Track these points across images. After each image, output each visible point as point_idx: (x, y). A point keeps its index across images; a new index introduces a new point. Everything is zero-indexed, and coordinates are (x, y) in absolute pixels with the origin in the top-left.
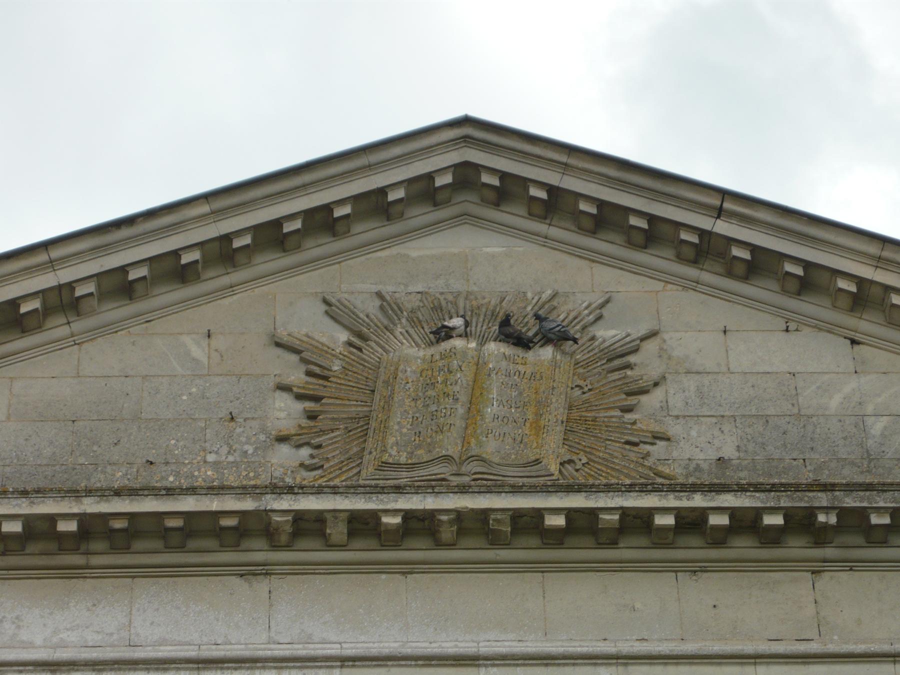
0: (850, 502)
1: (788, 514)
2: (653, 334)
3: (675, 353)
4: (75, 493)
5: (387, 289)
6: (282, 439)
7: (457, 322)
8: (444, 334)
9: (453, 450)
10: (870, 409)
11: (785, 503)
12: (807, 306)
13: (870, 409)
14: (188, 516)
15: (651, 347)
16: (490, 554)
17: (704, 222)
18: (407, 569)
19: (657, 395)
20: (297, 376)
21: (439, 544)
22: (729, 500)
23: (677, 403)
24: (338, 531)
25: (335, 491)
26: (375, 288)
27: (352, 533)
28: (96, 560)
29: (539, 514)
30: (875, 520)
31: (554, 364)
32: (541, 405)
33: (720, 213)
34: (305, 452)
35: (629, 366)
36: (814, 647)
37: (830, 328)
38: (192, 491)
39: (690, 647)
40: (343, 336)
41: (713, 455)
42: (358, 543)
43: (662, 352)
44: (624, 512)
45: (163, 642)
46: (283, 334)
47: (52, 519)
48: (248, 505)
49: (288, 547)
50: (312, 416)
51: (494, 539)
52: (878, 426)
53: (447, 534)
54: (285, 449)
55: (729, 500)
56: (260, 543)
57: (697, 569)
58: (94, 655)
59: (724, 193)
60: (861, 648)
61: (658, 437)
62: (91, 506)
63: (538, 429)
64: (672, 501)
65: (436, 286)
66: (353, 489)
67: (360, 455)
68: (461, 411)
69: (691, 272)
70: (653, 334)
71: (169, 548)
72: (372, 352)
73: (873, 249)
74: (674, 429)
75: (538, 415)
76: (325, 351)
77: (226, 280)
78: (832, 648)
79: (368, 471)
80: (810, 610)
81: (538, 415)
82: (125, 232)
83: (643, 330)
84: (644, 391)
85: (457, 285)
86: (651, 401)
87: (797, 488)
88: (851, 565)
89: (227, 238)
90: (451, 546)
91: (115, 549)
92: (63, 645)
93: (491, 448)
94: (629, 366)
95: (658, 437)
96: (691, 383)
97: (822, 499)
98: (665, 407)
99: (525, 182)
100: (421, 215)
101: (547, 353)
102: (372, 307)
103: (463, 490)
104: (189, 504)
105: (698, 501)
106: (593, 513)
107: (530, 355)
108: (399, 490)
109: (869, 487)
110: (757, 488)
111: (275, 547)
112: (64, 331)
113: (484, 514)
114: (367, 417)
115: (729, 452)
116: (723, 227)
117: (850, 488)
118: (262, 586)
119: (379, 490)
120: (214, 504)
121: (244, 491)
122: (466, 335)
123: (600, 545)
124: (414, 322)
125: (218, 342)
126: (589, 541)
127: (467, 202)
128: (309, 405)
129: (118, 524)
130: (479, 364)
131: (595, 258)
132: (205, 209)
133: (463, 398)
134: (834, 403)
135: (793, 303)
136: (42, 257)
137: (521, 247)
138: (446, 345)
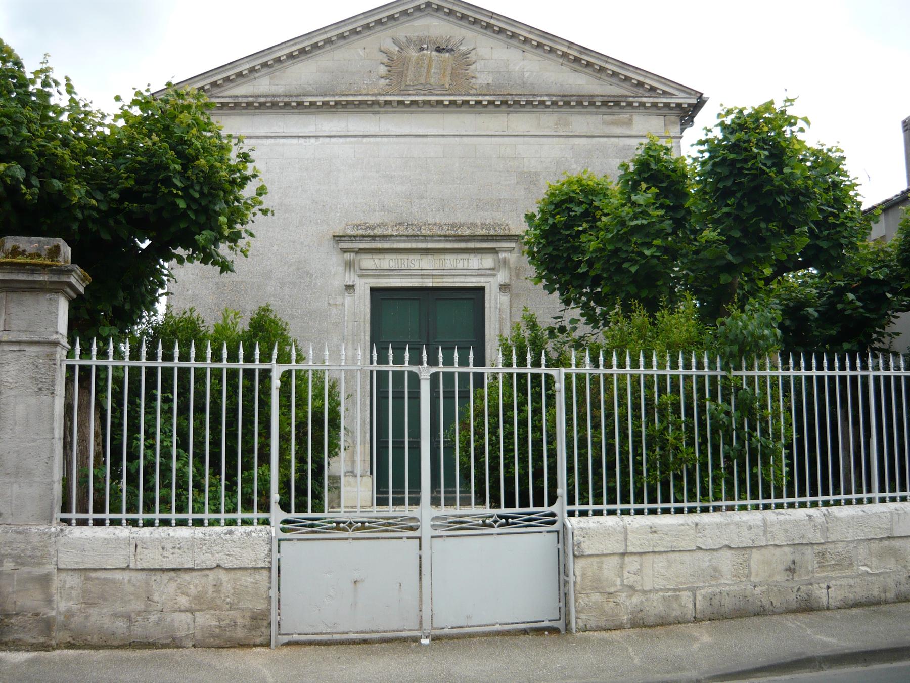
0: (516, 98)
1: (502, 102)
2: (474, 49)
3: (480, 54)
4: (333, 95)
5: (408, 35)
6: (382, 78)
7: (425, 46)
8: (422, 49)
9: (423, 82)
10: (525, 70)
11: (501, 99)
12: (513, 42)
13: (525, 70)
14: (360, 101)
15: (473, 52)
16: (431, 109)
17: (488, 20)
18: (412, 112)
19: (474, 66)
20: (385, 60)
21: (419, 107)
22: (488, 98)
23: (479, 68)
24: (395, 104)
25: (394, 95)
26: (404, 35)
27: (398, 104)
28: (339, 110)
29: (442, 101)
30: (522, 103)
31: (449, 58)
32: (446, 69)
33: (492, 17)
34: (388, 81)
35: (468, 58)
36: (505, 133)
37: (518, 47)
38: (361, 94)
39: (477, 133)
40: (397, 49)
41: (486, 82)
42: (400, 106)
43: (476, 54)
44: (463, 101)
45: (355, 130)
46: (382, 48)
47: (328, 102)
48: (374, 98)
49: (384, 107)
50: (389, 71)
51: (432, 106)
52: (527, 75)
53: (421, 105)
54: (383, 80)
55: (488, 98)
56: (377, 106)
57: (480, 113)
58: (340, 134)
59: (493, 13)
60: (516, 134)
61: (473, 77)
62: (337, 98)
63: (444, 76)
64: (474, 98)
65: (421, 34)
66: (398, 95)
67: (401, 82)
68: (425, 71)
69: (485, 31)
70: (474, 49)
71: (355, 107)
72: (404, 54)
73: (529, 29)
74: (478, 75)
75: (444, 72)
76: (392, 53)
77: (368, 33)
78: (509, 134)
79: (403, 87)
80: (506, 123)
81: (444, 72)
82: (343, 23)
83: (472, 47)
84: (471, 65)
85: (426, 34)
86: (473, 67)
87: (504, 95)
88: (516, 112)
89: (368, 24)
90: (422, 107)
91: (343, 108)
92: (332, 131)
93: (432, 81)
94: (468, 58)
95: (473, 77)
96: (482, 62)
97: (510, 98)
98: (476, 69)
99: (444, 7)
100: (417, 14)
101: (447, 55)
102: (404, 40)
103: (425, 95)
104: (360, 98)
105: (480, 98)
106: (455, 101)
107: (442, 55)
108: (409, 95)
109: (521, 95)
110: (495, 95)
111: (380, 107)
112: (329, 48)
113: (429, 101)
114: (403, 72)
115: (490, 82)
116: (492, 22)
117: (516, 95)
118: (378, 116)
119: (405, 95)
120: (365, 98)
121: (373, 95)
122: (427, 49)
123: (457, 107)
124: (415, 45)
125: (367, 50)
126: (455, 106)
127: (429, 10)
128: (389, 68)
129: (344, 103)
130: (431, 58)
131: (461, 26)
132: (362, 16)
133: (426, 68)
134: (517, 68)
135: (509, 41)
136: (323, 31)
137: (443, 23)
138: (422, 52)
